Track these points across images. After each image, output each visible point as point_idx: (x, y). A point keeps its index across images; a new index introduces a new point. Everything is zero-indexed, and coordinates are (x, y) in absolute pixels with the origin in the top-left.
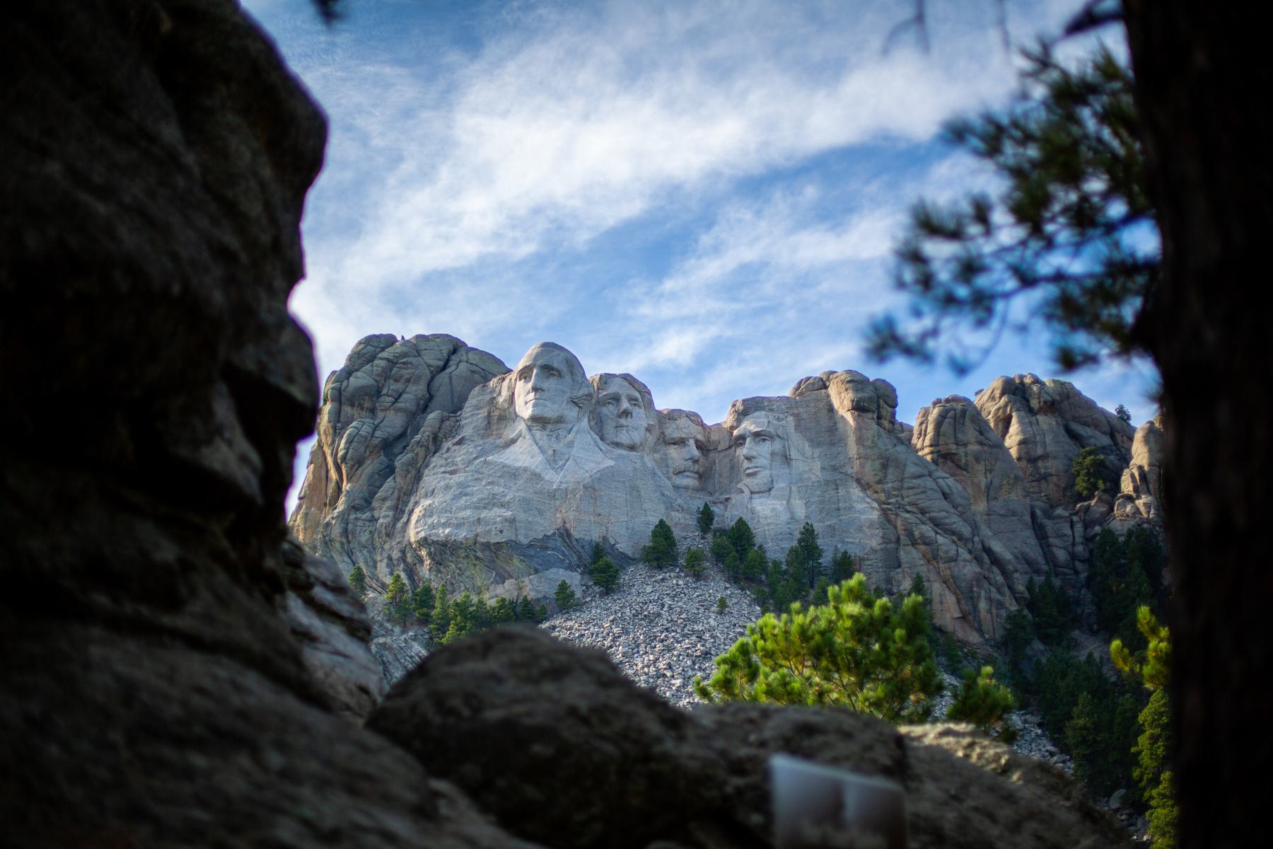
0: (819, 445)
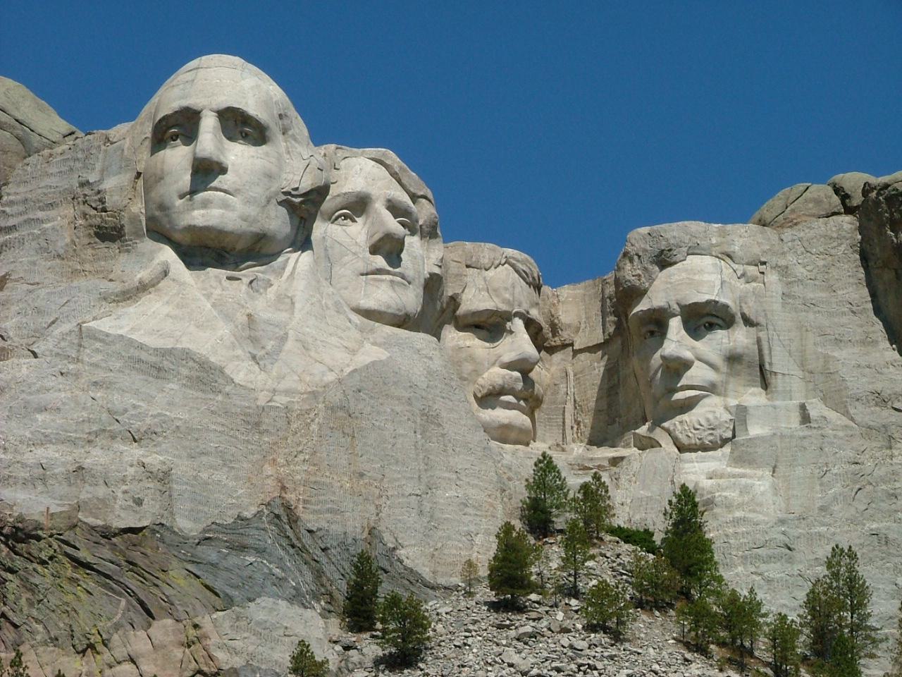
0: (838, 342)
